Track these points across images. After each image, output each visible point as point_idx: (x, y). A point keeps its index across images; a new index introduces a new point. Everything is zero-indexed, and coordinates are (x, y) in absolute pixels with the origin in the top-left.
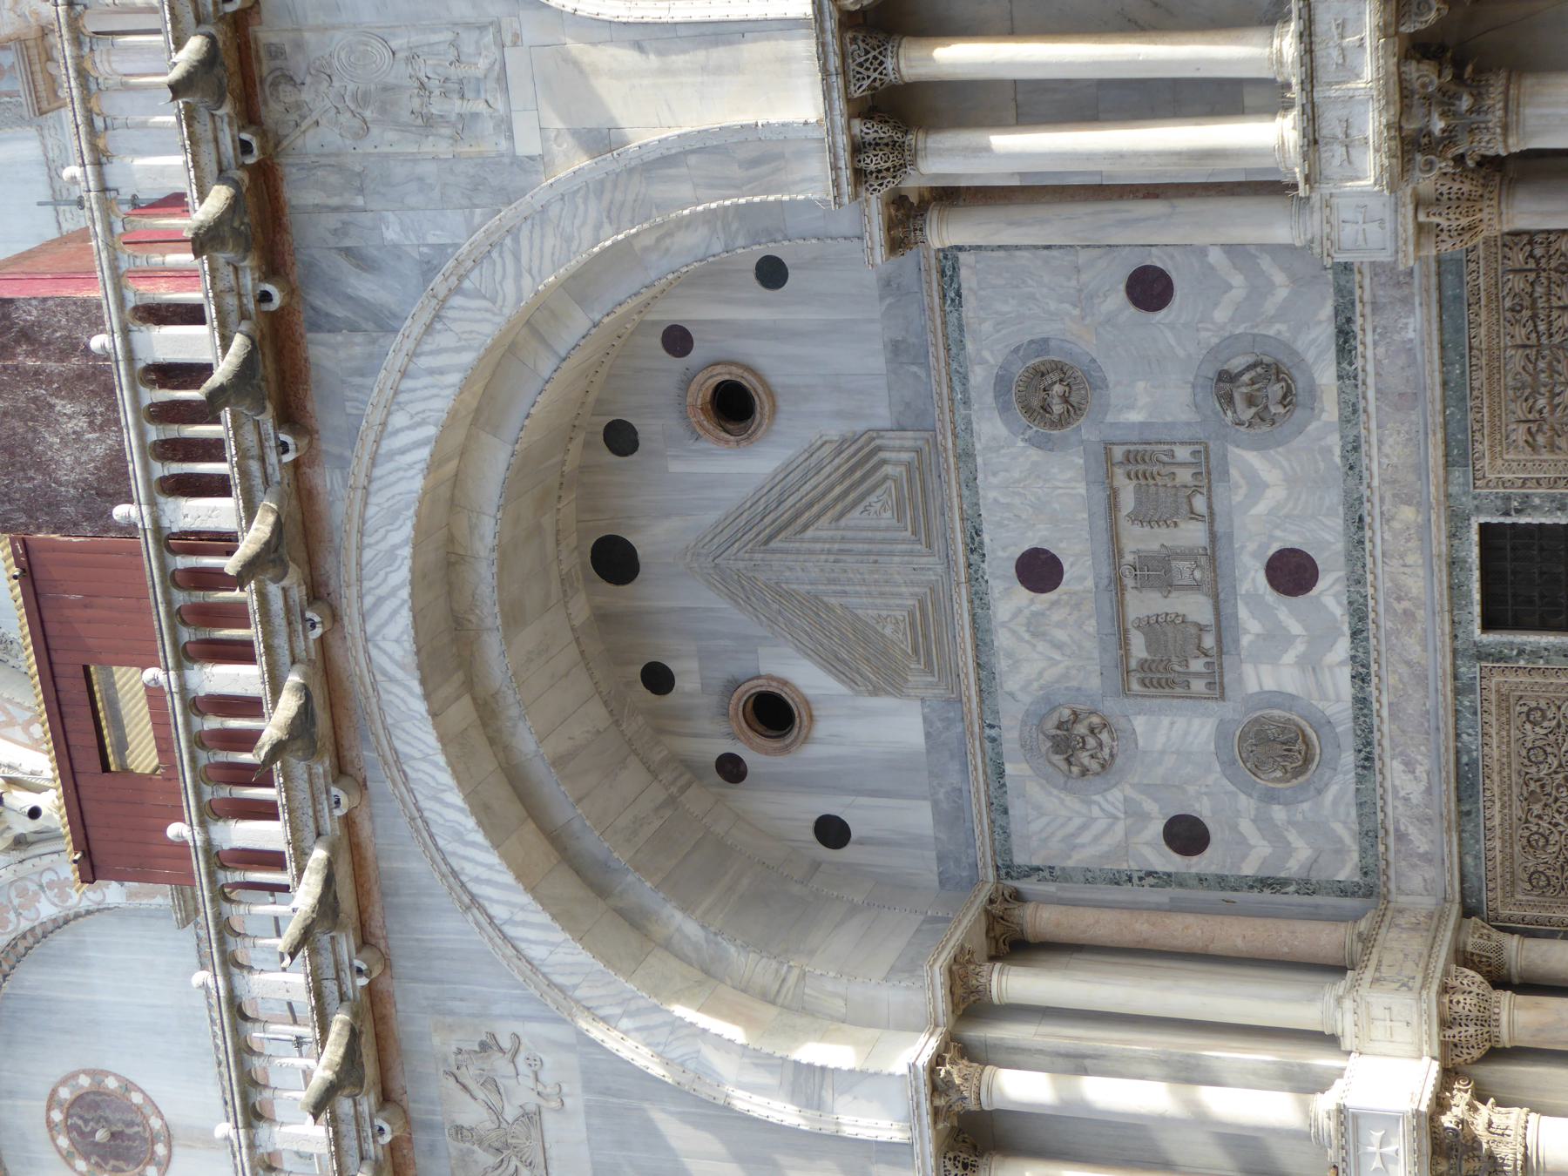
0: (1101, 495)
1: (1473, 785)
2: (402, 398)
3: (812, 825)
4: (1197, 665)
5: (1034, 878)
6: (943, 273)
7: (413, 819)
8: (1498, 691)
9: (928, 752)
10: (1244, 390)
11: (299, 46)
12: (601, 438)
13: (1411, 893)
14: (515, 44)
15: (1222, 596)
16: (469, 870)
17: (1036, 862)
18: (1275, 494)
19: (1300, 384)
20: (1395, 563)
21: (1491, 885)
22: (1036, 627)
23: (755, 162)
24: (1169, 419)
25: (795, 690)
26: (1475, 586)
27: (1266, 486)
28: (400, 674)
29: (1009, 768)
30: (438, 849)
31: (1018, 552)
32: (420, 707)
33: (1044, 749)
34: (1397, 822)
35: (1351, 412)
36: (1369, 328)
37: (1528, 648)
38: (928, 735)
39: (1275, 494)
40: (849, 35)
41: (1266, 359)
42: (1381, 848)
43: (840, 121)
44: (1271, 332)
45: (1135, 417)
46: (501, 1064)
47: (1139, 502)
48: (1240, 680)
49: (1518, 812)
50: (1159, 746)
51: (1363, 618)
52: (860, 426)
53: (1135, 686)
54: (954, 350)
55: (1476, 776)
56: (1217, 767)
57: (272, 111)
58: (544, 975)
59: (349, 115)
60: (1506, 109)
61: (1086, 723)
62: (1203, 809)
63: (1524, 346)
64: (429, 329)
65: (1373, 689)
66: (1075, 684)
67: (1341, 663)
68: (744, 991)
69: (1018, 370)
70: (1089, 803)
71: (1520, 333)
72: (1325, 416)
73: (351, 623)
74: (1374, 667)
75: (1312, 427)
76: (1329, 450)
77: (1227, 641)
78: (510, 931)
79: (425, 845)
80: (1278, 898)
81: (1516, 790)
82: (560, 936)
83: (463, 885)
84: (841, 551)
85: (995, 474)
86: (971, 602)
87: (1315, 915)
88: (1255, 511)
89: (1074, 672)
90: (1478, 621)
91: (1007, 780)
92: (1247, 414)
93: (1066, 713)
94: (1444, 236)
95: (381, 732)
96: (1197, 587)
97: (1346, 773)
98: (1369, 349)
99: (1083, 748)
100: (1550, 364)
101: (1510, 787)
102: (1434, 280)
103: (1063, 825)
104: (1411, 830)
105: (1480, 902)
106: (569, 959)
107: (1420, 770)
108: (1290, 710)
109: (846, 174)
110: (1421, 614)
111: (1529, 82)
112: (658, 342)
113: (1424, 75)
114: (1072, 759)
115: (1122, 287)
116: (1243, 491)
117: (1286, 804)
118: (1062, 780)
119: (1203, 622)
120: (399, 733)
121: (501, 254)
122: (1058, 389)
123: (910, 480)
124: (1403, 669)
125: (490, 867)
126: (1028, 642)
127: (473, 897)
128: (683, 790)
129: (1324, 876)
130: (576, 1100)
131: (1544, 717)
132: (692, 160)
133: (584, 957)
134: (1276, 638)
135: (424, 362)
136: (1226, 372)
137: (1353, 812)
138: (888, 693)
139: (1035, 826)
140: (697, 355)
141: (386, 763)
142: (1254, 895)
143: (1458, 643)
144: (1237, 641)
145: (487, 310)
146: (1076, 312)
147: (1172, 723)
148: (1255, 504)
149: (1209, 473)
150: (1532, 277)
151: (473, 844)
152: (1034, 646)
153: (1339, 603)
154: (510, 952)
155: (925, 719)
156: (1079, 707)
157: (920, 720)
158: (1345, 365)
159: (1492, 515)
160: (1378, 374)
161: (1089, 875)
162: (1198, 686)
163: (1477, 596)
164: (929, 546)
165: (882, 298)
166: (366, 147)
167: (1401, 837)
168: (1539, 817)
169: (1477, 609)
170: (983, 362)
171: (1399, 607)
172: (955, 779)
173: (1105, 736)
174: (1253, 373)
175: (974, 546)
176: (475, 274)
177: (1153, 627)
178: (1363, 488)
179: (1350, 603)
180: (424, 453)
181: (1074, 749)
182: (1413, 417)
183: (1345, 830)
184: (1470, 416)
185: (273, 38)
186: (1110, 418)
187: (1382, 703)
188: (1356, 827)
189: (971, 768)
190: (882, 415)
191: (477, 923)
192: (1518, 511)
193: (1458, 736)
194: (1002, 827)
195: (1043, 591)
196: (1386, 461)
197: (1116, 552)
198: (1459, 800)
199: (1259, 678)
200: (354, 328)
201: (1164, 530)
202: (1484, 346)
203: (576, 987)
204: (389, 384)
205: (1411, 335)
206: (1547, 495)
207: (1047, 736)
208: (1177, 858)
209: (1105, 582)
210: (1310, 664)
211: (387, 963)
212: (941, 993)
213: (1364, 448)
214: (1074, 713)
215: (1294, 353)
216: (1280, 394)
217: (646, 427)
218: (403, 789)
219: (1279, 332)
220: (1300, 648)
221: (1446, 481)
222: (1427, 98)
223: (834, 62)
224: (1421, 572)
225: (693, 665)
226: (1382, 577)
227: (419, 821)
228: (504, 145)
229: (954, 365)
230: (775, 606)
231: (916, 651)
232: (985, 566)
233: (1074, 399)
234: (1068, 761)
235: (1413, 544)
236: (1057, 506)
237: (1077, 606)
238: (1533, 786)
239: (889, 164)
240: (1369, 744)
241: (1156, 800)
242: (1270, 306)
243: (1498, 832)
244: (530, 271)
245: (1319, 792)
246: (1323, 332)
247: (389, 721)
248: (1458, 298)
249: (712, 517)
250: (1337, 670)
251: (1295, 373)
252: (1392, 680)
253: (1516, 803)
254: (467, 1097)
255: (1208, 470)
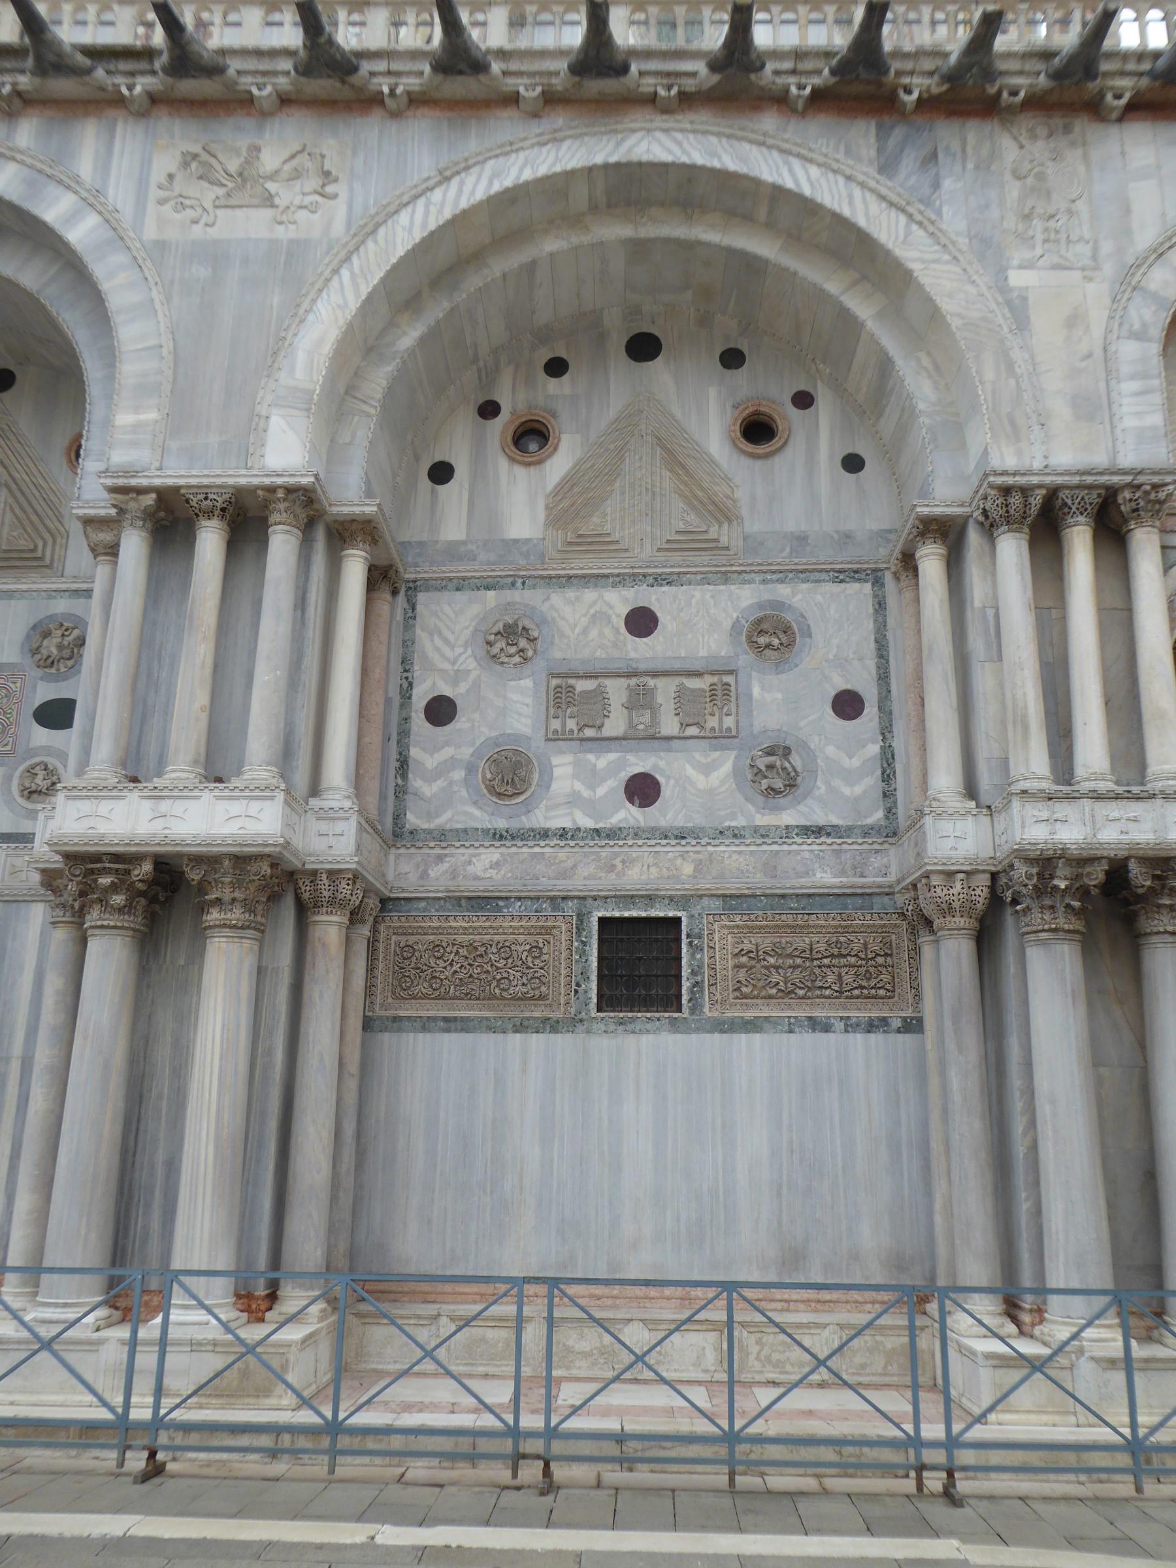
0: (698, 666)
1: (481, 909)
2: (831, 175)
3: (447, 459)
4: (571, 724)
5: (406, 606)
6: (856, 572)
7: (511, 144)
8: (554, 927)
9: (503, 540)
10: (778, 763)
11: (1073, 144)
12: (732, 346)
13: (396, 865)
14: (1085, 277)
15: (624, 742)
16: (470, 179)
17: (419, 608)
18: (701, 781)
19: (781, 801)
20: (651, 860)
21: (403, 919)
22: (600, 618)
23: (1013, 423)
24: (755, 713)
25: (550, 456)
26: (635, 914)
27: (707, 775)
28: (623, 149)
29: (491, 593)
30: (486, 160)
31: (655, 608)
32: (599, 159)
33: (507, 618)
34: (452, 855)
35: (762, 833)
36: (823, 847)
37: (587, 948)
38: (516, 541)
39: (701, 781)
40: (1103, 492)
41: (799, 779)
42: (432, 844)
43: (1048, 480)
44: (819, 783)
45: (756, 691)
46: (313, 183)
47: (693, 691)
48: (561, 752)
49: (460, 939)
50: (510, 695)
51: (608, 836)
52: (745, 512)
53: (554, 682)
54: (802, 576)
55: (488, 911)
56: (494, 734)
57: (1026, 122)
58: (385, 221)
59: (1029, 167)
60: (1069, 931)
61: (528, 647)
62: (460, 723)
63: (811, 950)
64: (883, 198)
65: (555, 842)
66: (557, 640)
67: (574, 821)
68: (356, 374)
69: (788, 617)
70: (466, 646)
71: (822, 947)
72: (758, 816)
73: (663, 121)
74: (572, 843)
75: (751, 808)
76: (734, 818)
77: (590, 744)
78: (421, 202)
79: (490, 150)
80: (392, 772)
81: (477, 938)
82: (418, 236)
83: (458, 173)
84: (654, 494)
85: (712, 597)
86: (618, 575)
87: (383, 797)
88: (688, 767)
89: (566, 641)
90: (608, 915)
91: (483, 592)
92: (761, 763)
93: (536, 634)
94: (945, 890)
95: (579, 131)
96: (631, 725)
97: (490, 822)
98: (809, 848)
99: (508, 644)
100: (799, 966)
101: (479, 934)
102: (859, 891)
103: (448, 627)
104: (446, 865)
105: (390, 911)
106: (399, 241)
107: (493, 872)
108: (538, 785)
109: (1010, 480)
110: (613, 876)
111: (1079, 948)
112: (802, 387)
113: (1096, 875)
114: (499, 636)
115: (849, 687)
116: (703, 760)
117: (465, 779)
118: (483, 629)
119: (603, 730)
120: (578, 143)
121: (935, 252)
122: (776, 642)
123: (707, 541)
124: (569, 864)
125: (473, 192)
126: (588, 612)
127: (448, 179)
128: (479, 370)
129: (410, 804)
130: (280, 232)
131: (535, 957)
132: (1012, 382)
133: (401, 251)
134: (593, 777)
135: (857, 192)
136: (790, 753)
137: (459, 826)
138: (547, 517)
139: (447, 609)
140: (794, 413)
141: (555, 131)
142: (394, 755)
143: (590, 901)
144: (590, 751)
145: (897, 238)
146: (831, 656)
147: (527, 705)
148: (693, 767)
149: (716, 738)
150: (862, 955)
151: (491, 183)
152: (585, 615)
153: (620, 821)
154: (405, 199)
155: (529, 540)
156: (539, 643)
157: (527, 537)
158: (796, 831)
159: (687, 926)
160: (790, 852)
161: (409, 643)
162: (556, 724)
163: (626, 914)
164: (659, 550)
165: (837, 532)
166: (1008, 176)
167: (440, 858)
168: (457, 953)
169: (617, 914)
170: (794, 594)
171: (617, 862)
172: (483, 556)
173: (517, 659)
174: (790, 770)
175: (659, 580)
176: (921, 233)
177: (600, 695)
178: (705, 841)
179: (620, 829)
180: (789, 184)
181: (507, 638)
182: (758, 875)
183: (444, 820)
184: (760, 913)
185: (1077, 129)
186: (754, 674)
187: (546, 849)
188: (448, 827)
189: (493, 567)
190: (754, 525)
191: (428, 178)
192: (690, 943)
193: (519, 899)
194: (446, 586)
195: (626, 624)
196: (727, 855)
197: (655, 674)
198: (469, 898)
199: (564, 765)
200: (880, 151)
201: (673, 706)
202: (811, 923)
203: (376, 242)
204: (843, 167)
205: (819, 875)
206: (703, 963)
207: (517, 620)
208: (423, 704)
209: (634, 665)
210: (574, 800)
211: (395, 115)
212: (357, 510)
213: (737, 841)
214: (535, 639)
215: (805, 798)
216: (776, 786)
217: (740, 376)
218: (535, 141)
219: (819, 788)
220: (586, 793)
221: (712, 895)
222: (1078, 877)
223: (1089, 479)
224: (643, 877)
225: (567, 390)
226: (641, 852)
227: (509, 148)
228: (1015, 262)
229: (791, 575)
230: (612, 447)
231: (580, 536)
232: (645, 586)
233: (767, 652)
234: (499, 633)
235: (665, 872)
236: (690, 636)
237: (615, 646)
238: (482, 949)
239: (1012, 512)
240: (513, 838)
241: (468, 691)
242: (837, 783)
243: (445, 925)
244: (925, 269)
245: (475, 803)
246: (820, 817)
247: (586, 139)
248: (845, 907)
249: (678, 413)
250: (569, 818)
251: (790, 798)
252: (562, 855)
253: (467, 938)
254: (286, 154)
255: (720, 738)
